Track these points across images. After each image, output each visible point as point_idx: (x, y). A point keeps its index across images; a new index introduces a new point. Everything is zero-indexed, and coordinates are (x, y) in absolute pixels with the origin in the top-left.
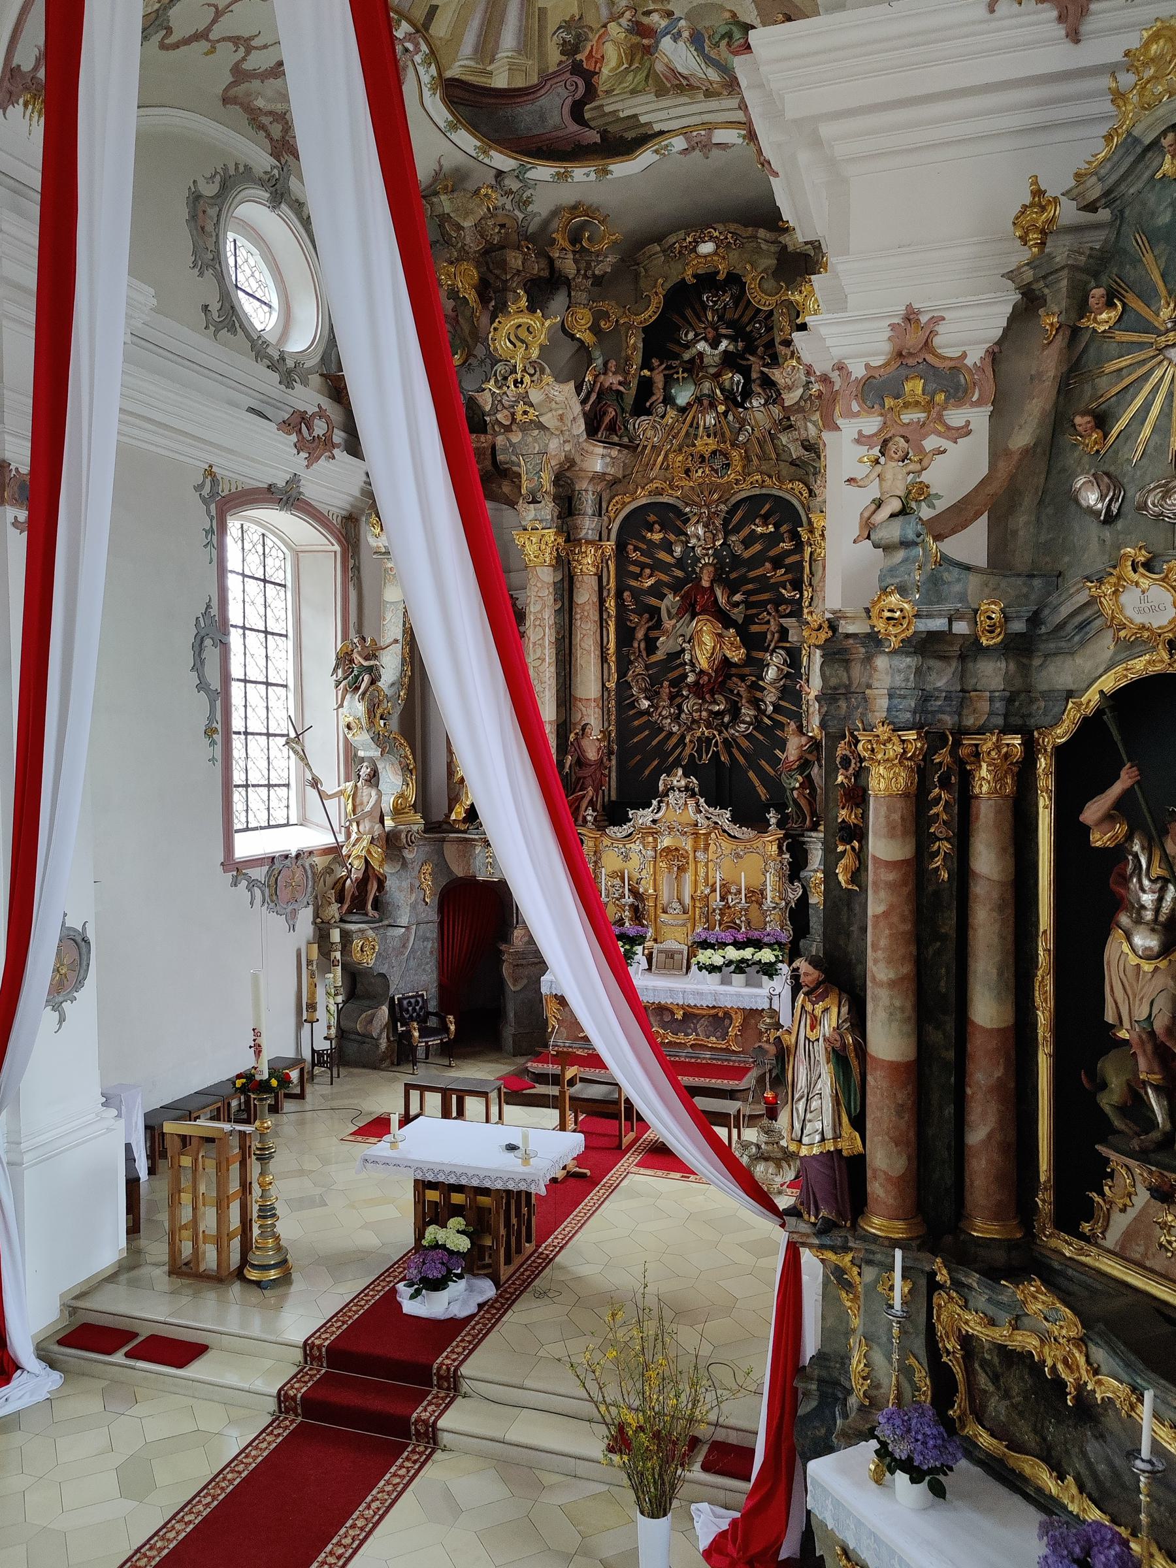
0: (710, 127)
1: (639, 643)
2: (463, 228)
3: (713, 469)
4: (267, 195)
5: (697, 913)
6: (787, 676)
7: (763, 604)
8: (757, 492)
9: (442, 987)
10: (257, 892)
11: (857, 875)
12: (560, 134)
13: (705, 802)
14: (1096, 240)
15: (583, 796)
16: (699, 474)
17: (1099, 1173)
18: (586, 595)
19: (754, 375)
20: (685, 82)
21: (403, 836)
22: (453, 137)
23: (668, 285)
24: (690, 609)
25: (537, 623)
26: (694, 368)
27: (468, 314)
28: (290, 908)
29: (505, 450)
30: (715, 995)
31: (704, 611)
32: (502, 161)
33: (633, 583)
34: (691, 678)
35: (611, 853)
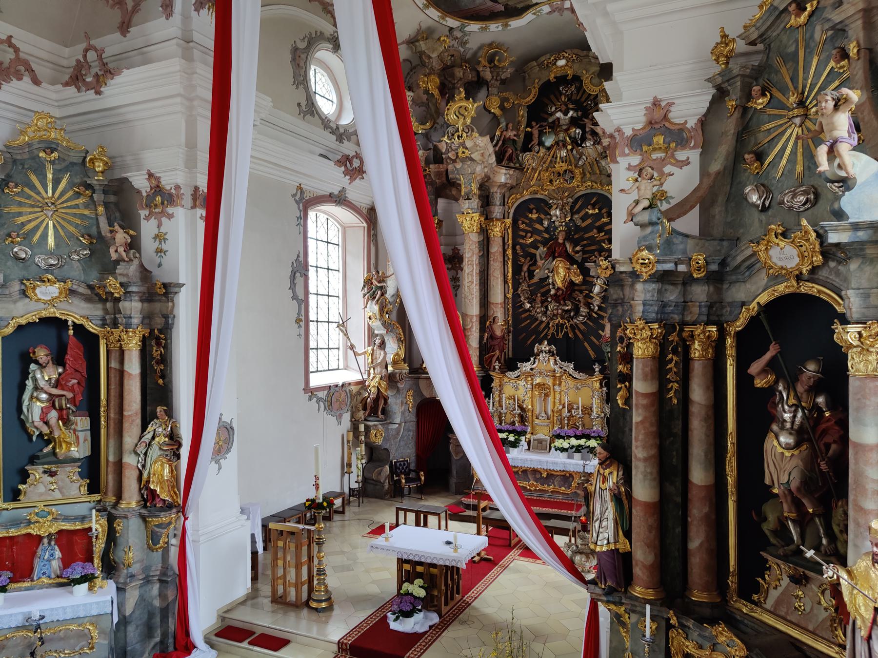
1: (524, 273)
3: (565, 180)
4: (331, 46)
7: (592, 252)
8: (589, 191)
9: (418, 457)
10: (322, 404)
11: (628, 401)
12: (482, 7)
14: (756, 61)
15: (494, 355)
16: (558, 182)
17: (762, 568)
18: (496, 248)
19: (587, 130)
21: (397, 375)
22: (427, 12)
23: (540, 83)
24: (552, 254)
26: (555, 126)
27: (434, 101)
28: (338, 413)
29: (453, 172)
30: (564, 464)
31: (559, 256)
32: (452, 22)
33: (522, 241)
34: (553, 292)
35: (508, 386)
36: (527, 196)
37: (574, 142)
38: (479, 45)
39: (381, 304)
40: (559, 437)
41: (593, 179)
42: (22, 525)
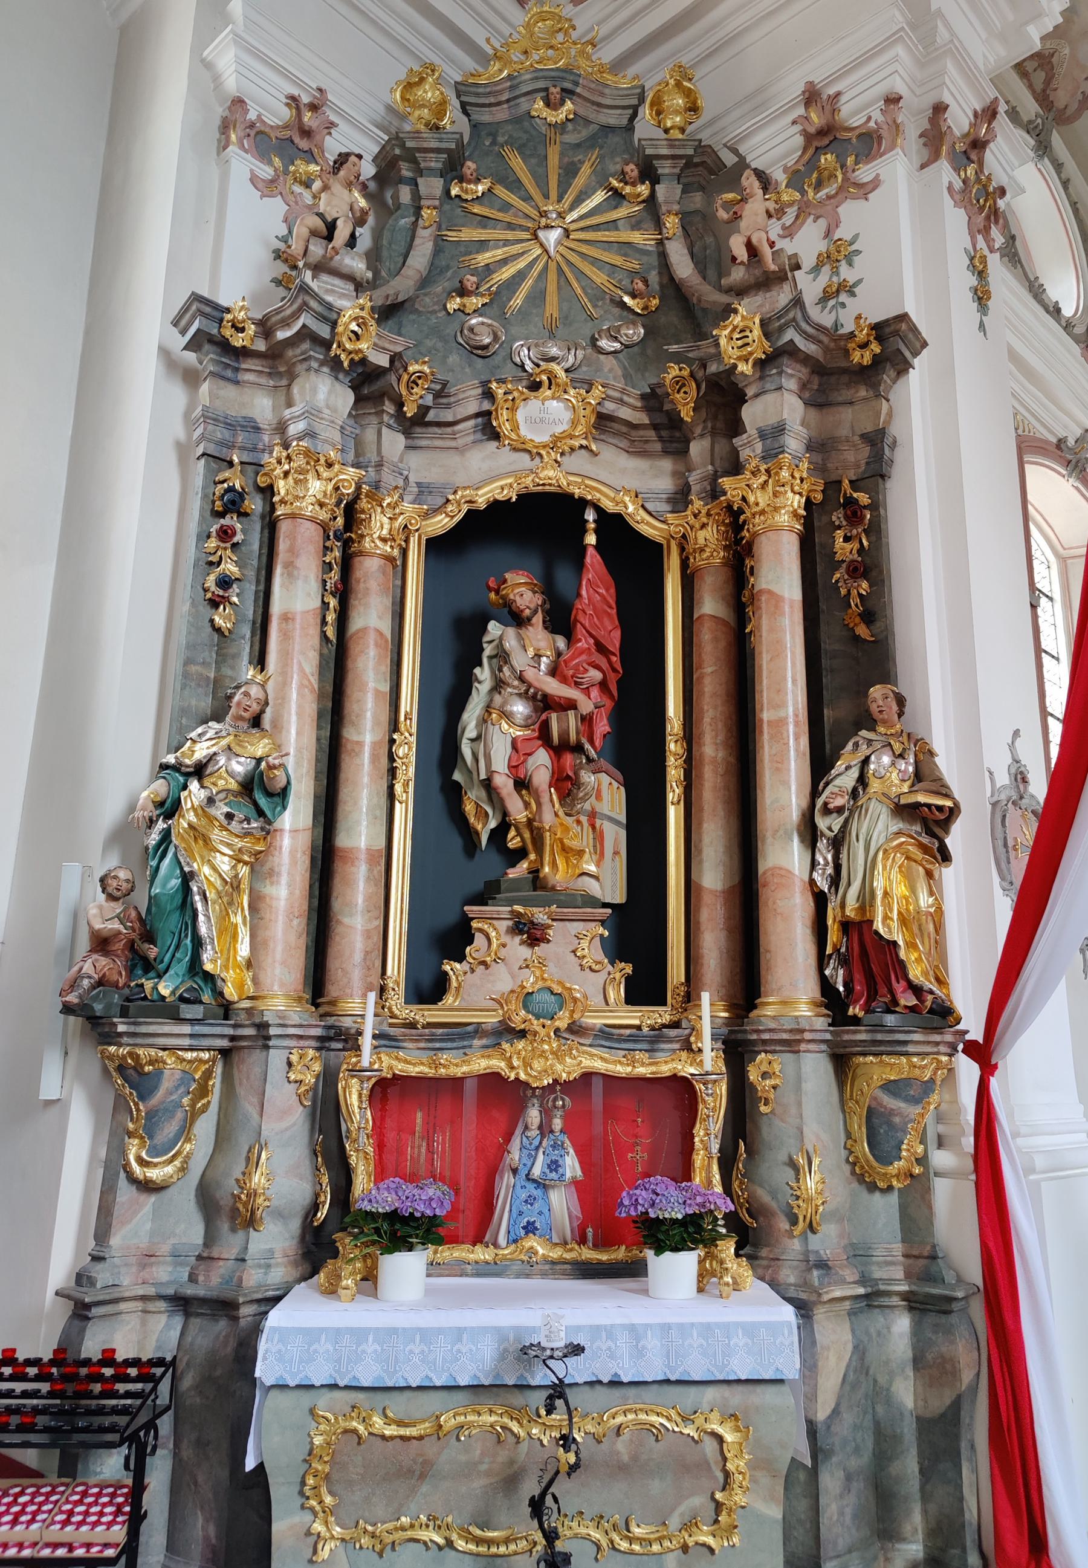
4: (1033, 142)
42: (477, 1042)
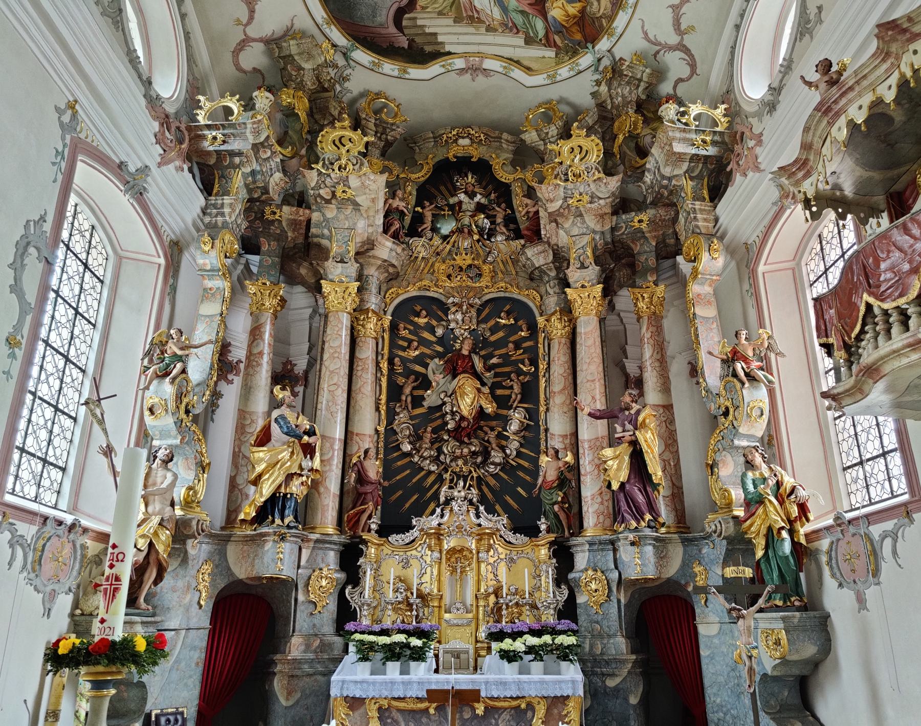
0: (483, 56)
2: (303, 69)
5: (481, 612)
6: (525, 428)
7: (507, 375)
8: (502, 294)
10: (19, 552)
12: (383, 31)
13: (485, 509)
15: (364, 511)
16: (458, 278)
18: (367, 352)
19: (499, 220)
20: (476, 16)
21: (194, 523)
23: (436, 160)
24: (453, 371)
25: (336, 355)
27: (298, 127)
28: (49, 589)
29: (318, 225)
31: (463, 372)
33: (401, 353)
34: (451, 426)
35: (390, 561)
36: (413, 292)
37: (481, 231)
38: (362, 90)
39: (180, 387)
40: (499, 636)
41: (507, 280)
